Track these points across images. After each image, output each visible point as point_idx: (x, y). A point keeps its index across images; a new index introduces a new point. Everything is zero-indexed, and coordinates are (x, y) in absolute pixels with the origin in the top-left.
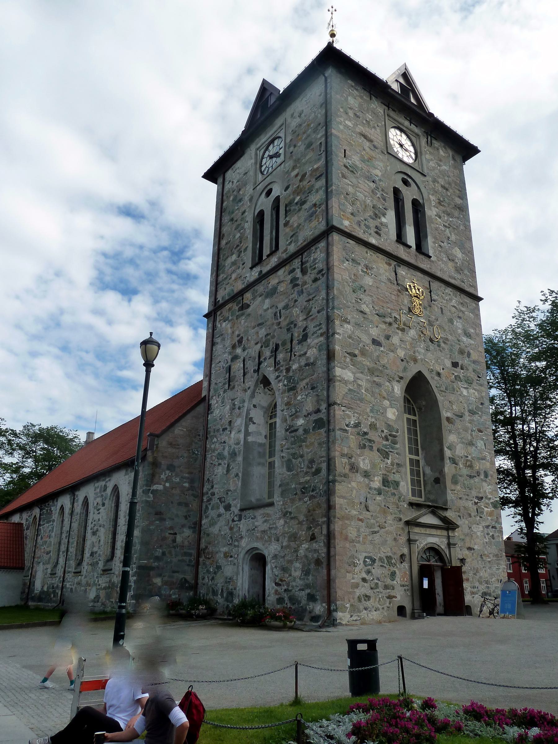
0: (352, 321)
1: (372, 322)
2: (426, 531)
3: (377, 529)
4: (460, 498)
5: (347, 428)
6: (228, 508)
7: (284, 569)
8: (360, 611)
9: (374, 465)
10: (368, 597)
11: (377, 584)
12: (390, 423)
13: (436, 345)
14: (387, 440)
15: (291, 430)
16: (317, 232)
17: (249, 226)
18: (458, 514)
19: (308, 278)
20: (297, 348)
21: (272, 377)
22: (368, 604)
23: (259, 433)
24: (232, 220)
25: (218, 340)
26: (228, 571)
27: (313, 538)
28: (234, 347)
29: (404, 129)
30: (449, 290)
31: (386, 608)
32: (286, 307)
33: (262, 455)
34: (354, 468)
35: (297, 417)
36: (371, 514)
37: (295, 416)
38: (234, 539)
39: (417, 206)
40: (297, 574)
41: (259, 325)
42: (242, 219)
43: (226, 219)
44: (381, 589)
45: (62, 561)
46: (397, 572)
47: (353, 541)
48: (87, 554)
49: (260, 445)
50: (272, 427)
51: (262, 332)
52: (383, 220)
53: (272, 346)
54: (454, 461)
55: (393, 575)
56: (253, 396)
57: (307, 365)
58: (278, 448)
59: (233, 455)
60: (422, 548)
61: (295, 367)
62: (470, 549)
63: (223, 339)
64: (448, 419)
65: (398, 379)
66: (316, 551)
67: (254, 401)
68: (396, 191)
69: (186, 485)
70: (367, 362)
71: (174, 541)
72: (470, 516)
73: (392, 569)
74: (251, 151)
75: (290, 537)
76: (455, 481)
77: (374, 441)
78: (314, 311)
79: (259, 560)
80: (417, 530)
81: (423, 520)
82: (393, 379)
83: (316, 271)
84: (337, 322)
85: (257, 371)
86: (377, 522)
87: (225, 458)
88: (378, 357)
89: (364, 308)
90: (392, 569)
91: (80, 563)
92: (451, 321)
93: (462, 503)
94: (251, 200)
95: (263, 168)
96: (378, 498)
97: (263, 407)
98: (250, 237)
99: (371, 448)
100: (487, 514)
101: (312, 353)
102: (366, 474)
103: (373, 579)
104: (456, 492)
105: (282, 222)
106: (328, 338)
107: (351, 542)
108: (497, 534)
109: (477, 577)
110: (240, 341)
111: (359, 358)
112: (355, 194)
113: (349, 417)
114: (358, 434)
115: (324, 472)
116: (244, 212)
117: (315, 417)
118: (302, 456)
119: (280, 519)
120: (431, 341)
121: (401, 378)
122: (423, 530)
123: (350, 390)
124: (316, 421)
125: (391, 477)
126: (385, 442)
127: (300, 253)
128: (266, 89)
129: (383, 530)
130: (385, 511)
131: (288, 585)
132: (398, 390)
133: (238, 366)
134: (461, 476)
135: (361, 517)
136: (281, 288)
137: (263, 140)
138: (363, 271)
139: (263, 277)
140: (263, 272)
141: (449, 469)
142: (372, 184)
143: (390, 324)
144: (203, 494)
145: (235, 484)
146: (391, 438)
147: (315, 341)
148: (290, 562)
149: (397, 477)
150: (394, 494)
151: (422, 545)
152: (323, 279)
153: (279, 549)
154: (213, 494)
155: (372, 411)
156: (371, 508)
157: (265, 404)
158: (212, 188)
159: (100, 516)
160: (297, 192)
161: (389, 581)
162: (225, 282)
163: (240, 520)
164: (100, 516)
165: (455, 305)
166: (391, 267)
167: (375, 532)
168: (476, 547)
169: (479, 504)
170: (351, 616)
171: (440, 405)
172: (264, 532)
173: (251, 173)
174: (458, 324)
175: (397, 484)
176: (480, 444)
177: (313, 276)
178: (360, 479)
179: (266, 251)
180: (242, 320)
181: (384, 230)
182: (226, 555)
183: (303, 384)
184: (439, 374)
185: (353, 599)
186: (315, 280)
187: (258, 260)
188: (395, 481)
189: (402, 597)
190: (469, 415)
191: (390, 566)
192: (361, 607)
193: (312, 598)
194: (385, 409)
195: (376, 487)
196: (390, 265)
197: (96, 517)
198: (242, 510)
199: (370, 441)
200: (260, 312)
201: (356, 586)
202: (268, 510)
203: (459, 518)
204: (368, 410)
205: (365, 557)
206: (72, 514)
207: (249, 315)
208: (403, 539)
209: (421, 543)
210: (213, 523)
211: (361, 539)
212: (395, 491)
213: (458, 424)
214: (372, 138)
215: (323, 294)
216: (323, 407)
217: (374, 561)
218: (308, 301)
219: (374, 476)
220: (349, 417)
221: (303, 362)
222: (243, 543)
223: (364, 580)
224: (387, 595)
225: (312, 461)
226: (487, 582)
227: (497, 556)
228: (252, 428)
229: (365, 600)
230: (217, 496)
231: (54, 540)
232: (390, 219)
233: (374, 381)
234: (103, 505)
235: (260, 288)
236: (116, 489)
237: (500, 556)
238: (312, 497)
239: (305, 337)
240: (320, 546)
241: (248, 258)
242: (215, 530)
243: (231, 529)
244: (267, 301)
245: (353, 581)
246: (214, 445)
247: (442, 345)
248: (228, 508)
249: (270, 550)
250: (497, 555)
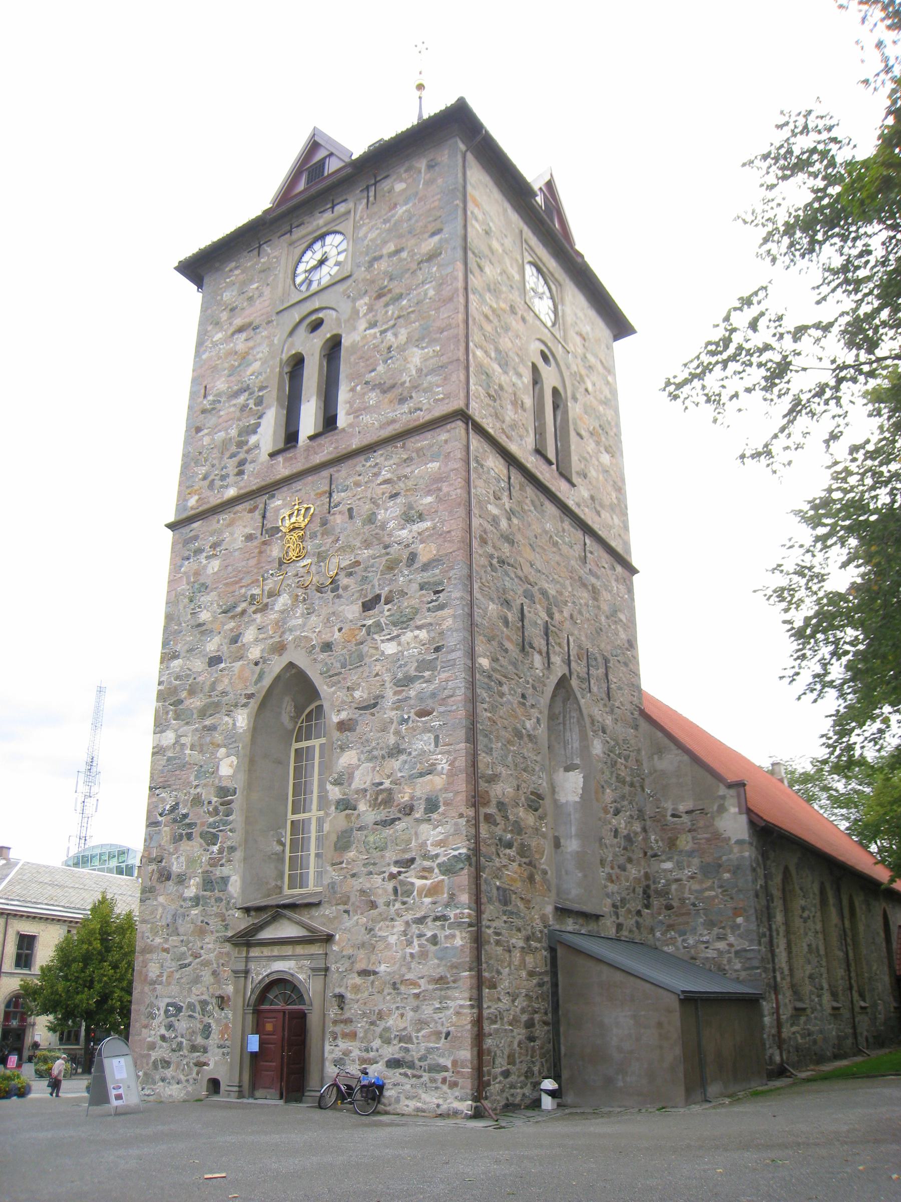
2: (272, 950)
4: (353, 876)
5: (160, 819)
8: (154, 1083)
9: (191, 861)
10: (166, 1064)
11: (181, 1043)
12: (224, 784)
13: (329, 592)
14: (216, 812)
18: (342, 908)
22: (169, 1073)
29: (324, 230)
30: (378, 457)
31: (191, 1081)
36: (181, 938)
44: (185, 1052)
46: (214, 1026)
47: (153, 983)
54: (346, 805)
55: (206, 1031)
60: (260, 982)
62: (364, 973)
64: (343, 726)
65: (246, 701)
70: (196, 703)
73: (207, 1020)
77: (195, 824)
82: (236, 706)
86: (189, 949)
88: (214, 683)
89: (205, 616)
90: (207, 1020)
92: (371, 519)
96: (194, 912)
99: (189, 836)
100: (420, 894)
103: (176, 1037)
104: (344, 865)
107: (151, 984)
108: (448, 932)
109: (378, 1030)
113: (163, 800)
114: (175, 821)
120: (319, 590)
121: (250, 696)
122: (267, 951)
125: (218, 872)
126: (211, 820)
129: (198, 960)
130: (201, 932)
132: (242, 720)
134: (360, 829)
135: (166, 946)
143: (244, 612)
149: (226, 871)
151: (261, 977)
155: (197, 777)
156: (181, 930)
161: (199, 1040)
165: (389, 476)
166: (257, 512)
167: (186, 966)
168: (382, 968)
169: (401, 877)
170: (143, 1089)
174: (390, 513)
175: (225, 880)
184: (327, 647)
185: (147, 1064)
188: (222, 878)
189: (218, 1064)
190: (395, 693)
191: (203, 1015)
192: (157, 1077)
195: (192, 895)
199: (190, 825)
201: (152, 1046)
203: (346, 915)
204: (192, 778)
205: (168, 1005)
208: (226, 973)
209: (258, 974)
211: (164, 978)
212: (221, 895)
213: (367, 725)
217: (179, 1009)
219: (190, 879)
223: (163, 1038)
224: (195, 1061)
226: (405, 1039)
227: (441, 980)
229: (163, 1067)
233: (205, 727)
237: (450, 979)
245: (149, 1039)
247: (344, 581)
250: (441, 978)
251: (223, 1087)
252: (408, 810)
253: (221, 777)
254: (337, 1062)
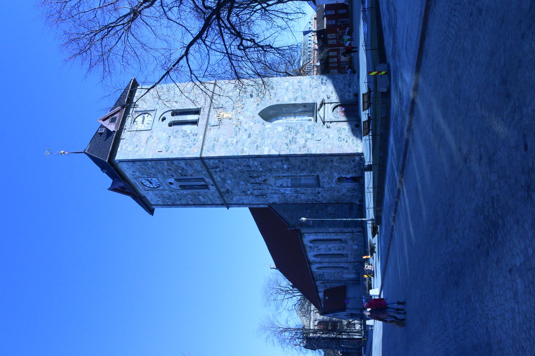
0: (242, 147)
1: (240, 138)
3: (327, 136)
6: (319, 193)
7: (344, 170)
9: (303, 137)
14: (291, 131)
15: (288, 169)
16: (201, 162)
17: (185, 192)
19: (221, 165)
20: (253, 169)
21: (264, 178)
23: (287, 182)
24: (180, 200)
25: (241, 202)
26: (344, 191)
27: (332, 161)
28: (246, 195)
32: (232, 174)
33: (296, 180)
34: (304, 147)
35: (283, 167)
37: (282, 169)
38: (331, 189)
39: (175, 113)
40: (345, 166)
41: (238, 184)
42: (181, 195)
43: (178, 203)
45: (342, 265)
48: (339, 252)
49: (292, 180)
50: (283, 176)
51: (242, 183)
52: (188, 132)
53: (250, 179)
54: (296, 99)
56: (271, 185)
57: (261, 165)
58: (295, 175)
59: (296, 192)
61: (261, 169)
63: (241, 199)
66: (337, 160)
67: (273, 184)
68: (170, 125)
69: (309, 211)
70: (259, 140)
71: (333, 214)
72: (318, 92)
74: (143, 192)
76: (304, 98)
78: (237, 162)
79: (340, 180)
80: (326, 118)
81: (322, 117)
83: (219, 163)
84: (244, 154)
85: (260, 184)
87: (297, 196)
89: (234, 142)
91: (342, 255)
93: (314, 96)
94: (172, 191)
95: (155, 187)
97: (275, 181)
98: (192, 191)
101: (256, 163)
102: (306, 141)
105: (190, 177)
106: (251, 158)
110: (244, 192)
111: (258, 144)
112: (180, 147)
115: (306, 158)
116: (178, 194)
117: (284, 162)
118: (300, 166)
121: (263, 124)
123: (273, 148)
124: (286, 161)
125: (306, 129)
127: (208, 170)
128: (113, 189)
132: (268, 125)
133: (256, 192)
136: (223, 176)
137: (141, 188)
138: (217, 142)
139: (215, 184)
140: (213, 183)
141: (300, 101)
142: (172, 138)
143: (239, 129)
144: (313, 203)
145: (309, 190)
146: (290, 128)
147: (251, 162)
148: (341, 168)
149: (306, 126)
150: (313, 128)
152: (223, 160)
154: (313, 199)
157: (274, 180)
158: (157, 210)
159: (323, 248)
160: (176, 171)
162: (212, 200)
163: (324, 188)
164: (323, 248)
171: (272, 105)
172: (329, 178)
173: (157, 192)
175: (309, 126)
176: (287, 84)
177: (221, 164)
178: (308, 143)
179: (203, 183)
180: (234, 192)
181: (193, 132)
182: (338, 192)
183: (269, 166)
186: (223, 163)
187: (206, 187)
193: (354, 161)
194: (278, 132)
196: (210, 129)
197: (323, 250)
198: (320, 187)
200: (232, 184)
202: (320, 177)
206: (320, 263)
207: (232, 189)
210: (325, 198)
214: (146, 137)
215: (230, 160)
216: (280, 158)
218: (232, 165)
220: (284, 148)
222: (334, 186)
223: (347, 142)
225: (302, 162)
226: (345, 84)
228: (285, 185)
230: (314, 197)
231: (332, 271)
232: (188, 128)
234: (318, 247)
235: (219, 185)
236: (312, 241)
238: (316, 162)
239: (248, 166)
240: (335, 159)
241: (202, 191)
242: (328, 197)
243: (328, 191)
244: (227, 182)
246: (291, 200)
248: (319, 193)
249: (336, 176)
251: (356, 123)
252: (300, 86)
253: (282, 131)
254: (350, 97)
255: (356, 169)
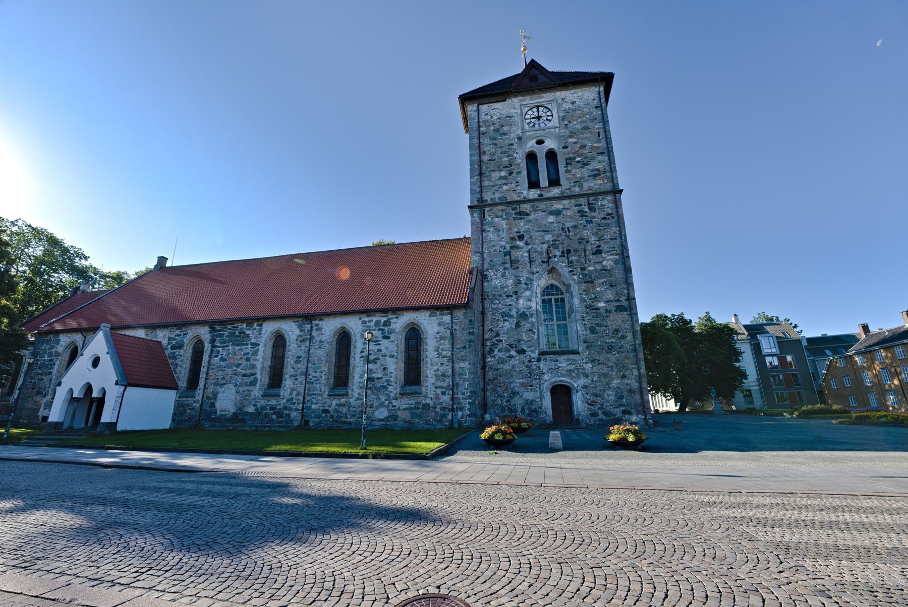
38: (532, 375)
75: (599, 376)
119: (587, 363)
131: (602, 405)
153: (589, 382)
163: (539, 360)
207: (530, 221)
221: (599, 267)
222: (546, 377)
225: (617, 331)
255: (601, 416)
